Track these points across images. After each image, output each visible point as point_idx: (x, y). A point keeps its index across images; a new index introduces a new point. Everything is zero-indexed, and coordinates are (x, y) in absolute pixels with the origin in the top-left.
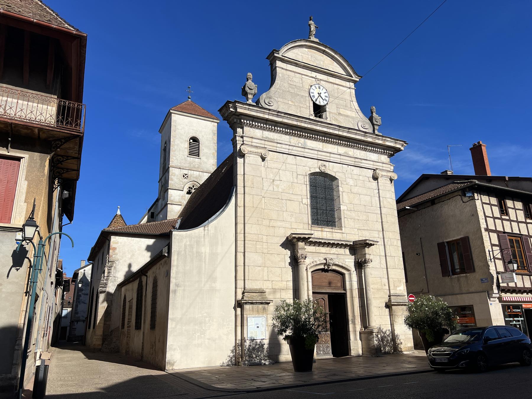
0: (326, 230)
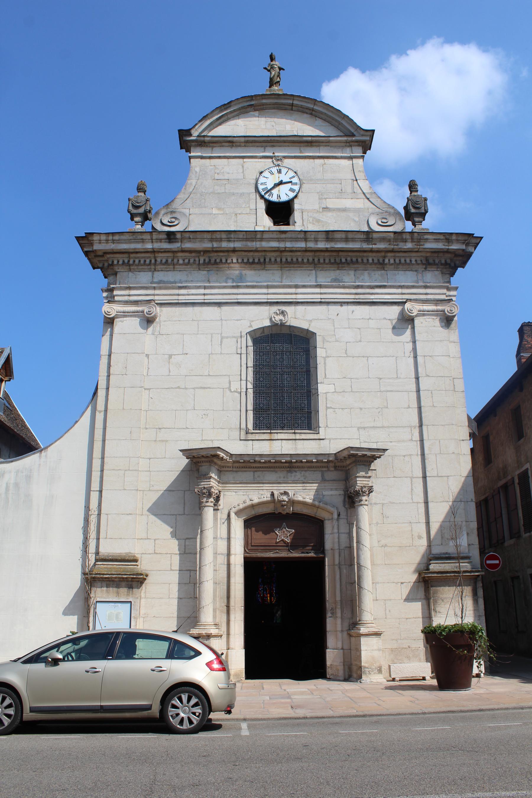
0: (280, 436)
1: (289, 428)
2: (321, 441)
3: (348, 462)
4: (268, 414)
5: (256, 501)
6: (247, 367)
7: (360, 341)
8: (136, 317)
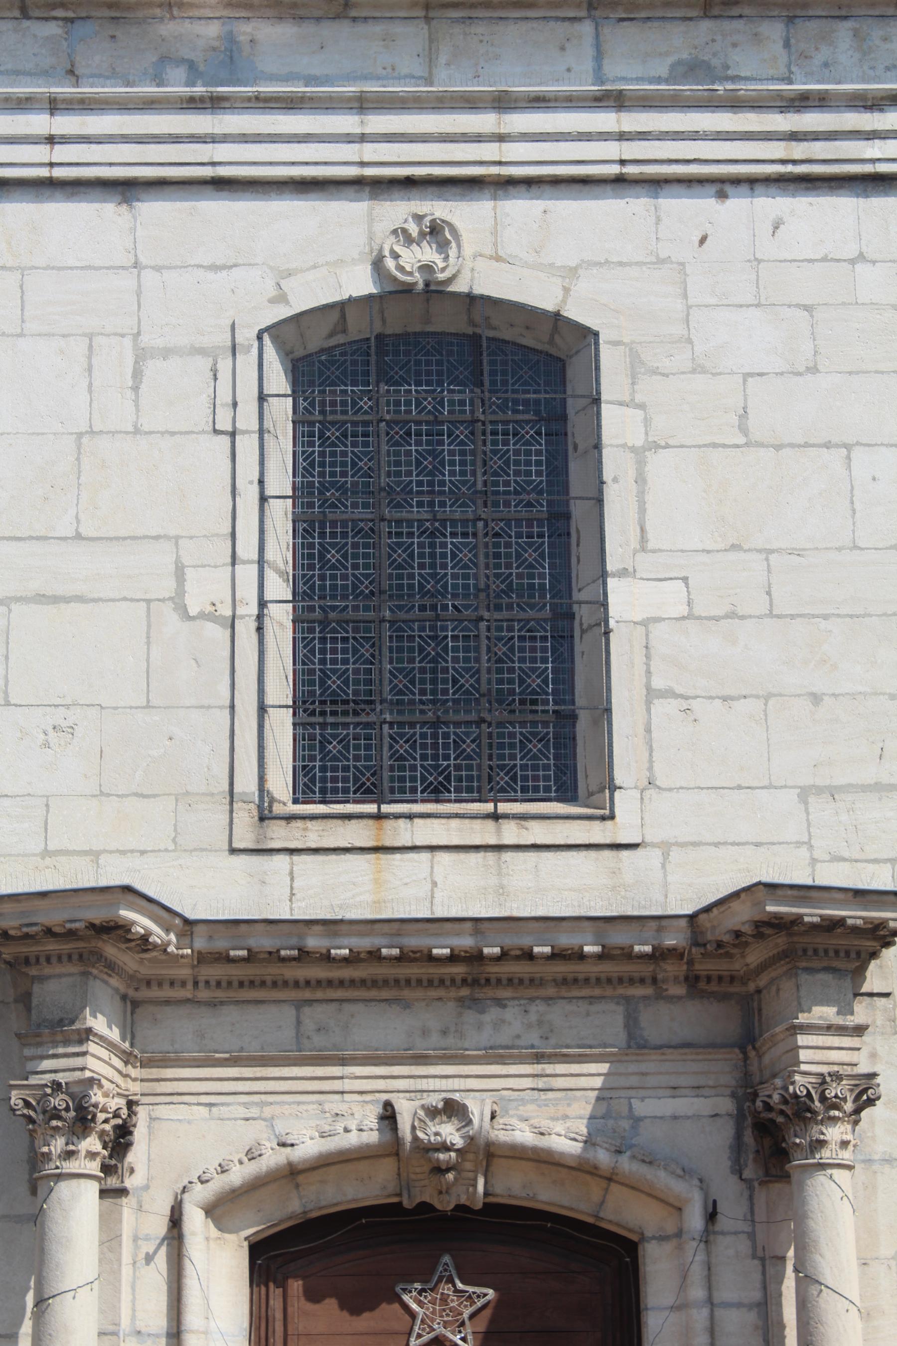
1: (470, 790)
2: (625, 854)
3: (755, 956)
4: (368, 725)
5: (309, 1147)
6: (263, 499)
7: (813, 369)
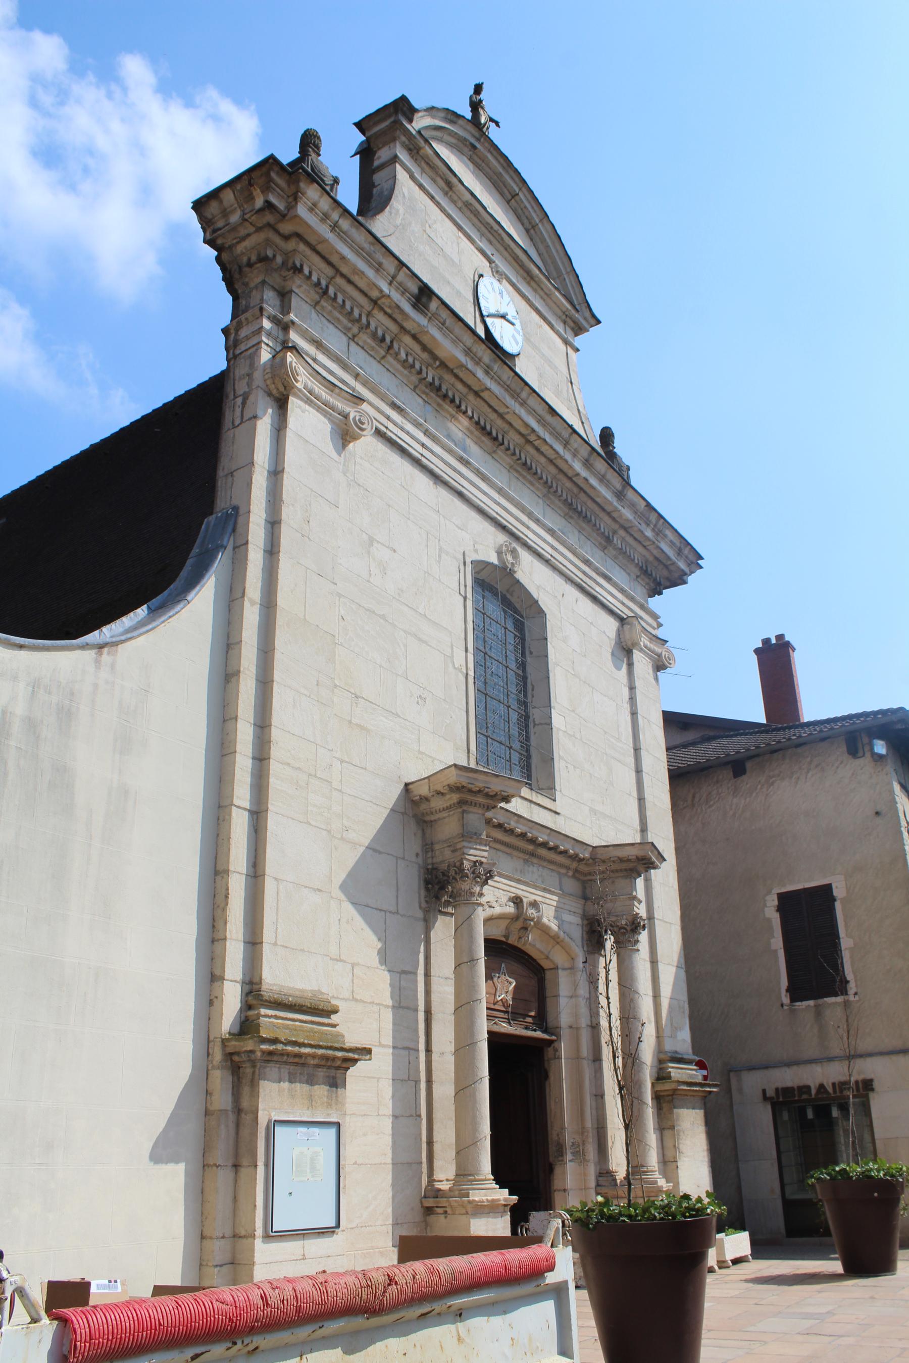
8: (325, 416)
